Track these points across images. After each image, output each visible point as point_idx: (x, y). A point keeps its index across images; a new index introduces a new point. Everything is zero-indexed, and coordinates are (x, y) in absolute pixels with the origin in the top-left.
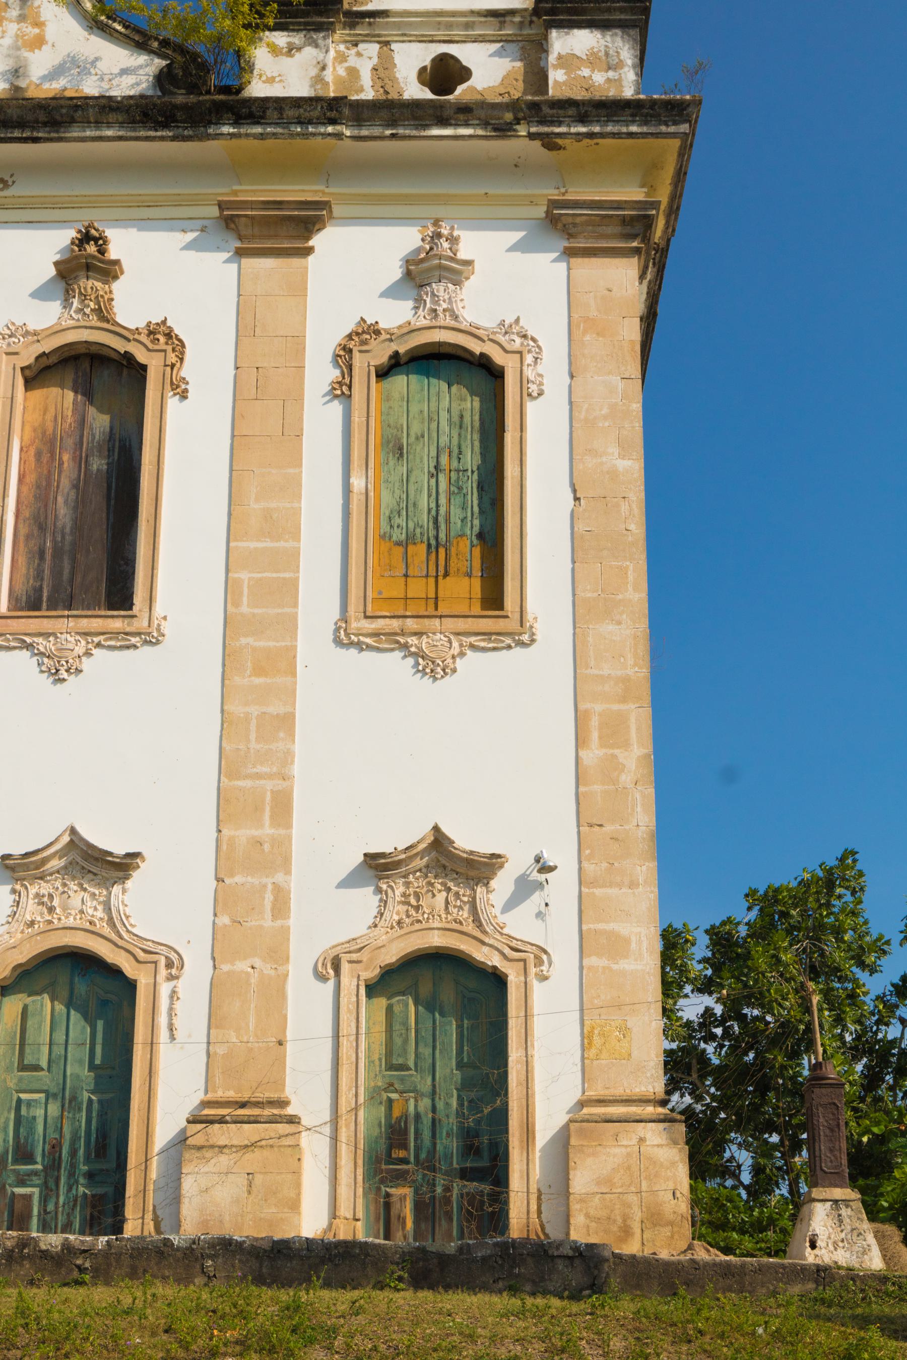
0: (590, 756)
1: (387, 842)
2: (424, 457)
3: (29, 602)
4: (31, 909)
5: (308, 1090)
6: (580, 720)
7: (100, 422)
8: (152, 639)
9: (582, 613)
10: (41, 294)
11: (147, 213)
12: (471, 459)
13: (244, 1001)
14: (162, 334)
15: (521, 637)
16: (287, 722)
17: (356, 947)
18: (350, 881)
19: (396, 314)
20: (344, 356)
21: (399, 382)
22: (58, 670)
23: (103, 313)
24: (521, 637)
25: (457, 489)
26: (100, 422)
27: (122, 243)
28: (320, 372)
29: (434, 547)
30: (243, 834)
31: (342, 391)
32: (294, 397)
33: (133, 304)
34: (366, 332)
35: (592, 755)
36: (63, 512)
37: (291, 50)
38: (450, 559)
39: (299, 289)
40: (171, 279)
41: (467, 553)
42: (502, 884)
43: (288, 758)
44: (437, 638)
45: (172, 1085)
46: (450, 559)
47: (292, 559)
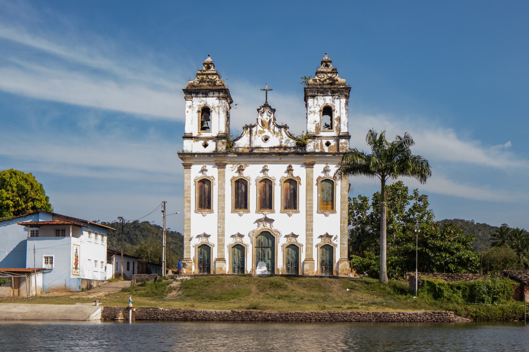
0: (342, 225)
1: (323, 234)
2: (326, 191)
3: (286, 208)
4: (289, 240)
5: (315, 257)
6: (341, 221)
7: (292, 187)
8: (299, 212)
9: (342, 210)
10: (285, 172)
11: (296, 163)
12: (331, 192)
13: (309, 249)
14: (298, 178)
15: (335, 212)
16: (312, 221)
17: (319, 244)
18: (319, 238)
19: (323, 175)
20: (317, 180)
21: (323, 183)
22: (290, 215)
23: (292, 175)
24: (335, 212)
25: (329, 195)
26: (292, 187)
27: (294, 166)
28: (315, 182)
29: (327, 202)
30: (308, 233)
31: (317, 184)
32: (312, 186)
33: (295, 174)
34: (320, 177)
35: (342, 225)
36: (289, 197)
37: (311, 142)
38: (327, 204)
39: (312, 172)
40: (299, 171)
41: (330, 202)
42: (333, 238)
43: (312, 225)
44: (327, 213)
45: (303, 257)
46: (327, 204)
47: (312, 204)
